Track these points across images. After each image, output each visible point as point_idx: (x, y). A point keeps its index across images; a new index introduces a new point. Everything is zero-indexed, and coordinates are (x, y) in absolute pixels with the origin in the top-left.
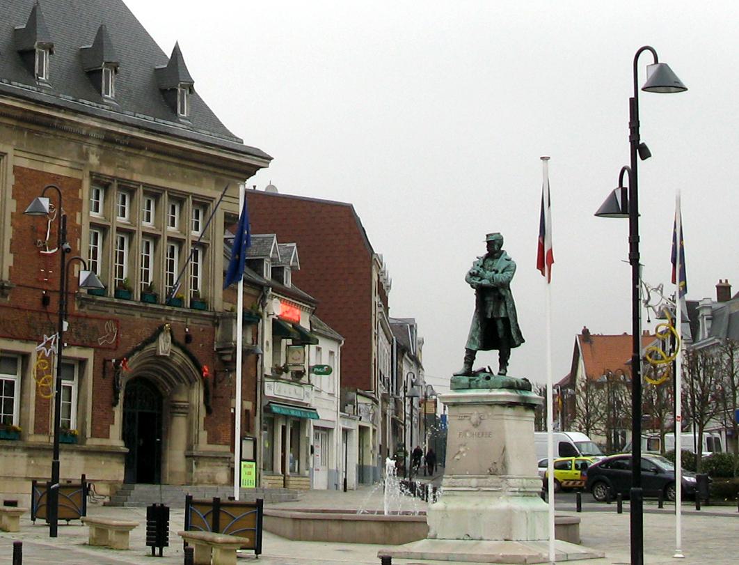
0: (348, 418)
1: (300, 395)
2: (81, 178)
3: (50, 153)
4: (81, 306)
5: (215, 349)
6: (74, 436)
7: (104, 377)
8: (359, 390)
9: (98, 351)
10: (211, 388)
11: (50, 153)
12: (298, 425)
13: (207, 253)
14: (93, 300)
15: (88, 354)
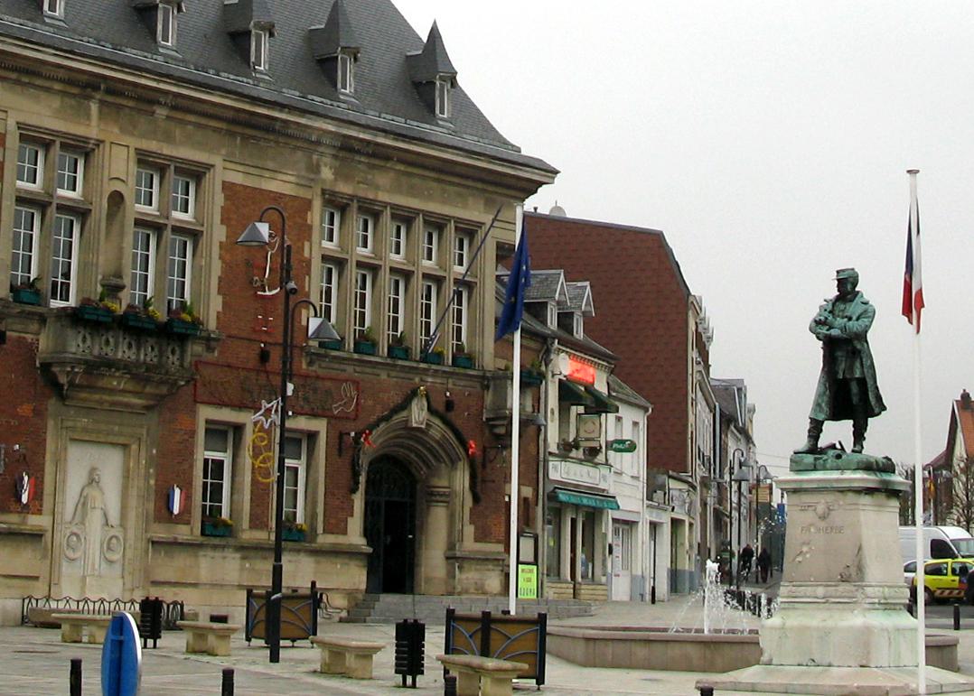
0: (658, 508)
1: (595, 478)
2: (310, 197)
3: (270, 165)
4: (310, 363)
5: (484, 419)
6: (301, 531)
7: (340, 455)
8: (671, 472)
9: (333, 421)
10: (479, 470)
11: (270, 165)
12: (592, 517)
13: (474, 295)
14: (326, 356)
15: (320, 426)
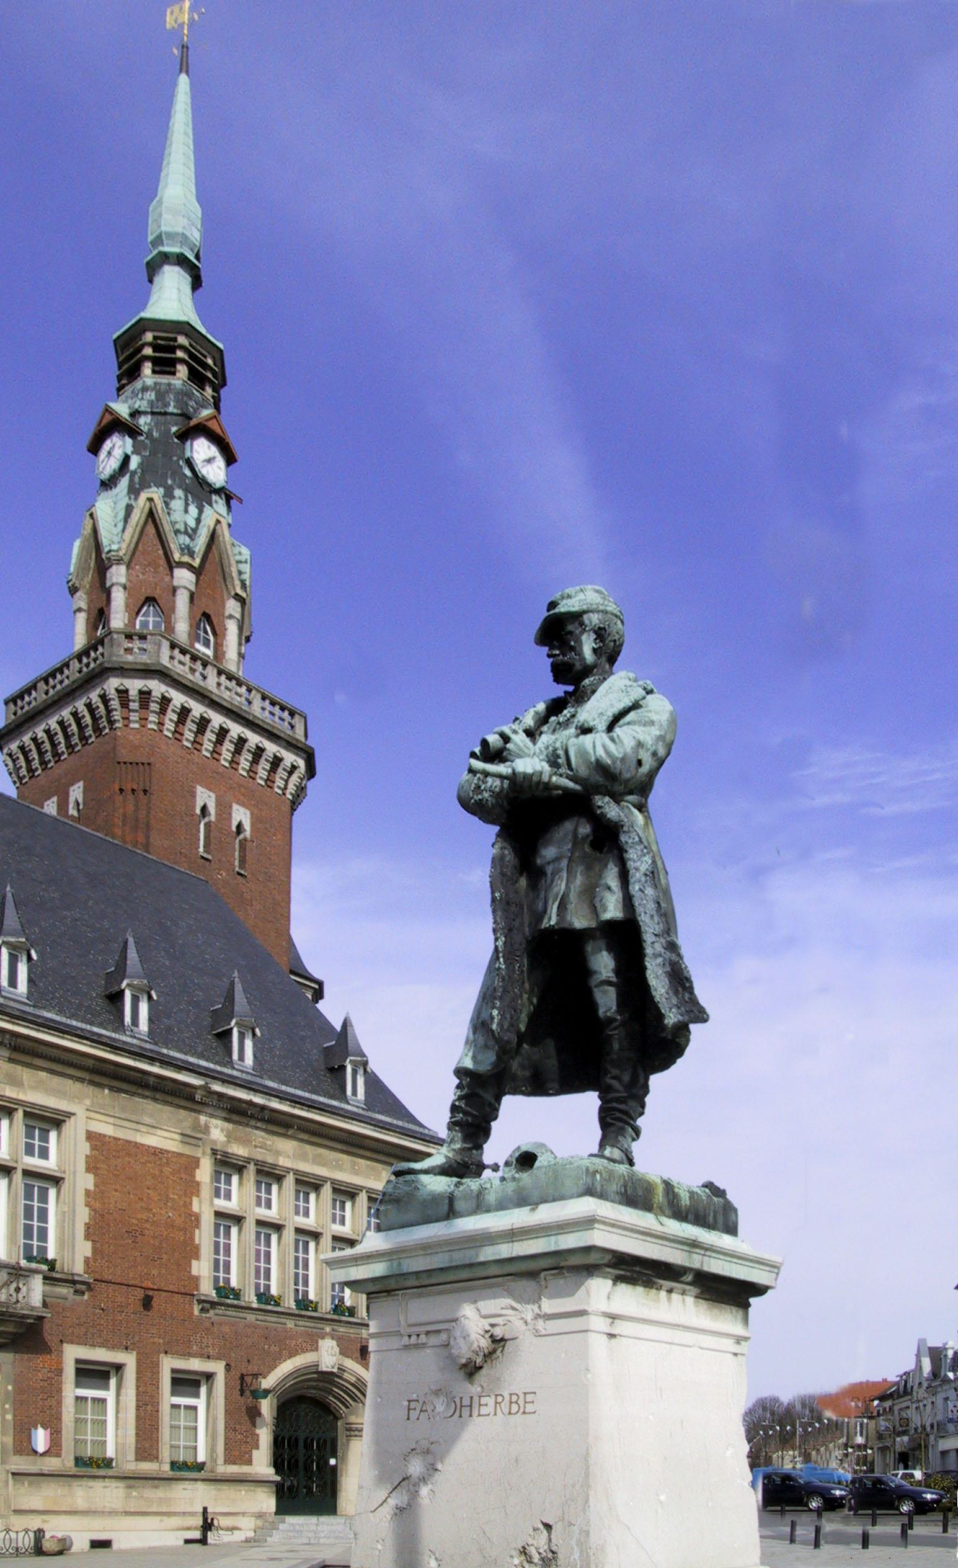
3: (147, 1120)
11: (147, 1120)
